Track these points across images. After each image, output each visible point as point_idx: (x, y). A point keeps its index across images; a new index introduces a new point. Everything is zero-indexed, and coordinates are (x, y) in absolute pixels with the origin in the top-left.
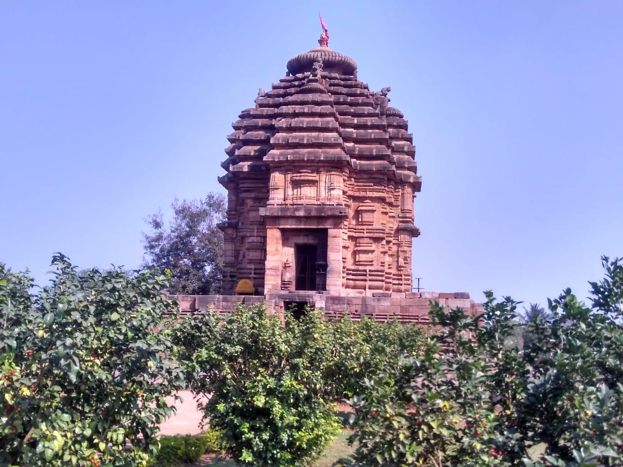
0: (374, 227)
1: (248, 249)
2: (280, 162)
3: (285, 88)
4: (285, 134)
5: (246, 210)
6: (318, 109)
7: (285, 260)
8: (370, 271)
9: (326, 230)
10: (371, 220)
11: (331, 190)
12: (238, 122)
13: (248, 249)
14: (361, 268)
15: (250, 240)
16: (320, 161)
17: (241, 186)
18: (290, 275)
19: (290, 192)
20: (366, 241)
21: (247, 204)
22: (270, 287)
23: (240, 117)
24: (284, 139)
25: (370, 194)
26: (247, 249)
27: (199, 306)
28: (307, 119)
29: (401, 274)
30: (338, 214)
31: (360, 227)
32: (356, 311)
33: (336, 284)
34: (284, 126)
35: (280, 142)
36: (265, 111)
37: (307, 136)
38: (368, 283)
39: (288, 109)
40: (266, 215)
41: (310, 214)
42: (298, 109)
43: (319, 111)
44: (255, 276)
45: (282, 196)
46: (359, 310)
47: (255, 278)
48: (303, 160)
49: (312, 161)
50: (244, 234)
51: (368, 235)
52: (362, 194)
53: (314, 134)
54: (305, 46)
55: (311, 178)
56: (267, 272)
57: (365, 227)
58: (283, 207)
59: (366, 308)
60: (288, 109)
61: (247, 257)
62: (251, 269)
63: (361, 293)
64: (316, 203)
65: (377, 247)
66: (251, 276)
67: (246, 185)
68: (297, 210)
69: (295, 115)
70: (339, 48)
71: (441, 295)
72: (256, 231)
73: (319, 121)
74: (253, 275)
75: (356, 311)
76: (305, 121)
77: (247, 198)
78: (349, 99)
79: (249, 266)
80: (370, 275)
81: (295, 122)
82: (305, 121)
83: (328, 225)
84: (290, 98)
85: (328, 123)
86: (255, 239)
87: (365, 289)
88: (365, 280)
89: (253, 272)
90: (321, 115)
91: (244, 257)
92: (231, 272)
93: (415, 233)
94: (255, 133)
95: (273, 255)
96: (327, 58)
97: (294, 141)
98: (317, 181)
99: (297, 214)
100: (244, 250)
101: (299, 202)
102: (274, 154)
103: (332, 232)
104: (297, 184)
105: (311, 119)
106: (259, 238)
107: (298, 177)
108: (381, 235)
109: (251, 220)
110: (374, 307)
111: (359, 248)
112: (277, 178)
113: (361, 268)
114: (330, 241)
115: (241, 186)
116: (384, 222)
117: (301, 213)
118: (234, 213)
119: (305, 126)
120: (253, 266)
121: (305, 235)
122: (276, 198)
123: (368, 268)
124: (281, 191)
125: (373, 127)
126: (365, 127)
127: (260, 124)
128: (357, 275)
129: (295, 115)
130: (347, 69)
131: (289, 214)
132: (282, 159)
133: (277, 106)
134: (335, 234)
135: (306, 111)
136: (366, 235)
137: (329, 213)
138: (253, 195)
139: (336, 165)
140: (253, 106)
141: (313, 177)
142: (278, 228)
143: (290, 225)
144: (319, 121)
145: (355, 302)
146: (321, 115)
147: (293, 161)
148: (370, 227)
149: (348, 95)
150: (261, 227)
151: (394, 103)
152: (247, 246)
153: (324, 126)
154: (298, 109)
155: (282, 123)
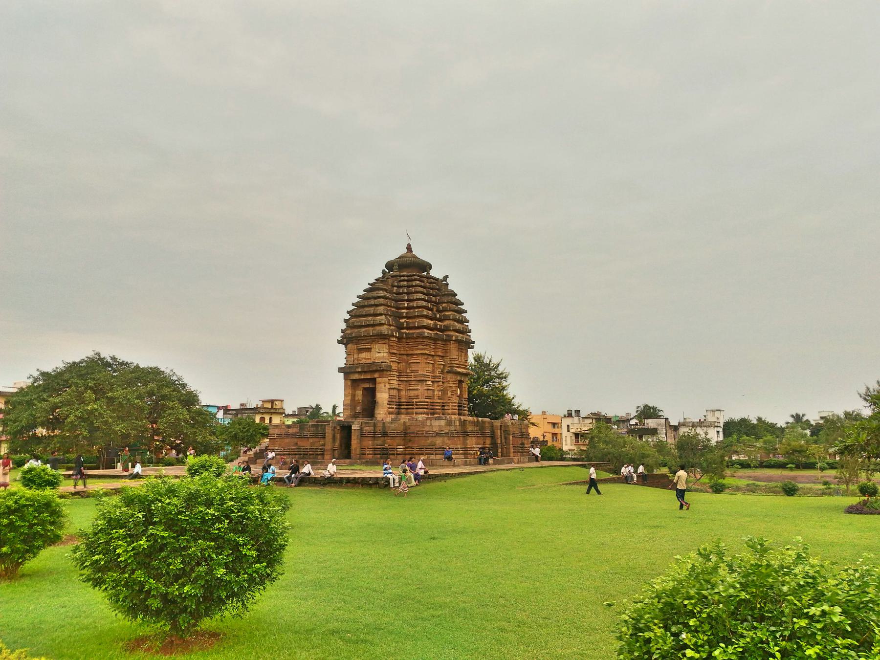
28: (367, 309)
38: (415, 411)
52: (411, 352)
68: (357, 367)
83: (376, 375)
104: (360, 351)
117: (360, 370)
139: (382, 337)
143: (356, 376)
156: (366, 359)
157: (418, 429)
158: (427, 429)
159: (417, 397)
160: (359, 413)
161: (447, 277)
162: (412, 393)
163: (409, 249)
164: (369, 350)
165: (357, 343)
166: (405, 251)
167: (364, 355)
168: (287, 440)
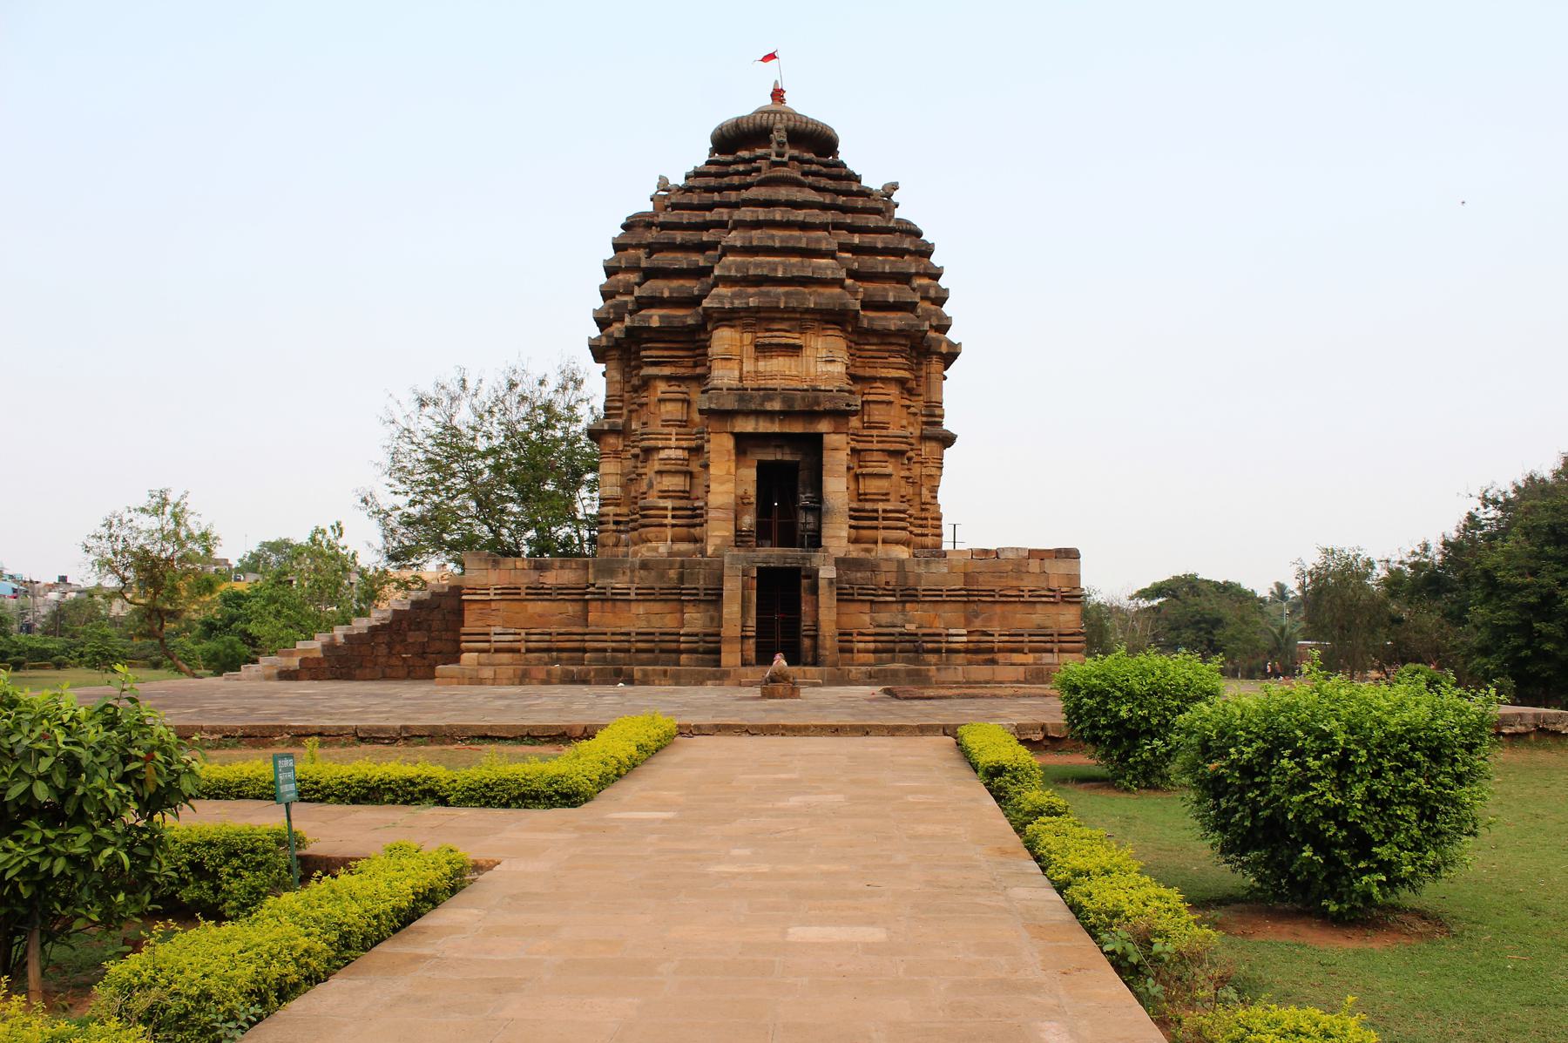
0: (890, 432)
1: (660, 473)
2: (733, 310)
3: (717, 175)
4: (739, 259)
5: (654, 399)
6: (800, 215)
7: (741, 492)
8: (885, 511)
9: (820, 436)
10: (885, 419)
11: (822, 363)
12: (621, 236)
13: (660, 473)
14: (868, 506)
15: (663, 454)
16: (808, 311)
17: (643, 353)
18: (748, 520)
19: (748, 366)
20: (877, 456)
22: (718, 541)
23: (623, 227)
24: (739, 267)
25: (885, 373)
27: (596, 578)
29: (927, 517)
30: (844, 407)
31: (865, 432)
32: (887, 583)
33: (837, 537)
34: (738, 244)
35: (733, 273)
36: (686, 216)
37: (782, 263)
38: (881, 534)
39: (746, 214)
42: (762, 214)
43: (800, 218)
45: (737, 374)
46: (893, 582)
47: (673, 526)
48: (777, 309)
49: (794, 310)
50: (652, 443)
51: (880, 446)
52: (868, 372)
53: (794, 260)
54: (747, 102)
55: (792, 341)
56: (712, 514)
57: (875, 432)
58: (741, 392)
59: (906, 578)
60: (746, 214)
61: (657, 487)
62: (666, 509)
63: (868, 550)
64: (800, 386)
65: (895, 467)
66: (665, 521)
68: (770, 399)
69: (757, 225)
70: (806, 104)
71: (1033, 553)
73: (802, 239)
75: (887, 583)
76: (778, 237)
77: (656, 377)
78: (841, 199)
79: (662, 503)
80: (884, 519)
81: (757, 237)
82: (778, 237)
83: (823, 426)
84: (745, 194)
85: (819, 240)
86: (673, 453)
87: (876, 542)
88: (876, 528)
89: (670, 514)
90: (804, 226)
91: (651, 486)
93: (948, 440)
94: (671, 255)
95: (722, 483)
96: (791, 124)
97: (759, 272)
98: (801, 347)
99: (768, 406)
100: (651, 474)
101: (771, 384)
102: (721, 297)
103: (831, 440)
104: (763, 350)
105: (787, 233)
106: (680, 454)
107: (765, 338)
108: (904, 447)
110: (919, 576)
111: (865, 471)
112: (723, 339)
113: (868, 506)
114: (828, 458)
115: (643, 353)
116: (904, 422)
118: (619, 404)
119: (777, 244)
120: (669, 504)
121: (777, 446)
122: (724, 375)
123: (881, 506)
124: (733, 360)
125: (886, 251)
126: (872, 251)
127: (679, 240)
128: (861, 517)
129: (757, 225)
130: (820, 142)
131: (753, 407)
132: (737, 303)
133: (709, 207)
134: (837, 445)
135: (778, 217)
136: (876, 446)
137: (829, 406)
138: (667, 371)
140: (649, 207)
141: (793, 339)
144: (802, 239)
145: (884, 567)
146: (804, 226)
147: (758, 309)
148: (884, 432)
149: (838, 192)
150: (682, 430)
151: (906, 210)
152: (657, 467)
153: (813, 246)
154: (762, 214)
155: (735, 238)
156: (784, 377)
157: (1004, 582)
158: (1028, 584)
159: (885, 497)
160: (749, 533)
161: (895, 187)
162: (872, 486)
163: (778, 95)
164: (794, 350)
165: (746, 327)
166: (767, 101)
167: (779, 367)
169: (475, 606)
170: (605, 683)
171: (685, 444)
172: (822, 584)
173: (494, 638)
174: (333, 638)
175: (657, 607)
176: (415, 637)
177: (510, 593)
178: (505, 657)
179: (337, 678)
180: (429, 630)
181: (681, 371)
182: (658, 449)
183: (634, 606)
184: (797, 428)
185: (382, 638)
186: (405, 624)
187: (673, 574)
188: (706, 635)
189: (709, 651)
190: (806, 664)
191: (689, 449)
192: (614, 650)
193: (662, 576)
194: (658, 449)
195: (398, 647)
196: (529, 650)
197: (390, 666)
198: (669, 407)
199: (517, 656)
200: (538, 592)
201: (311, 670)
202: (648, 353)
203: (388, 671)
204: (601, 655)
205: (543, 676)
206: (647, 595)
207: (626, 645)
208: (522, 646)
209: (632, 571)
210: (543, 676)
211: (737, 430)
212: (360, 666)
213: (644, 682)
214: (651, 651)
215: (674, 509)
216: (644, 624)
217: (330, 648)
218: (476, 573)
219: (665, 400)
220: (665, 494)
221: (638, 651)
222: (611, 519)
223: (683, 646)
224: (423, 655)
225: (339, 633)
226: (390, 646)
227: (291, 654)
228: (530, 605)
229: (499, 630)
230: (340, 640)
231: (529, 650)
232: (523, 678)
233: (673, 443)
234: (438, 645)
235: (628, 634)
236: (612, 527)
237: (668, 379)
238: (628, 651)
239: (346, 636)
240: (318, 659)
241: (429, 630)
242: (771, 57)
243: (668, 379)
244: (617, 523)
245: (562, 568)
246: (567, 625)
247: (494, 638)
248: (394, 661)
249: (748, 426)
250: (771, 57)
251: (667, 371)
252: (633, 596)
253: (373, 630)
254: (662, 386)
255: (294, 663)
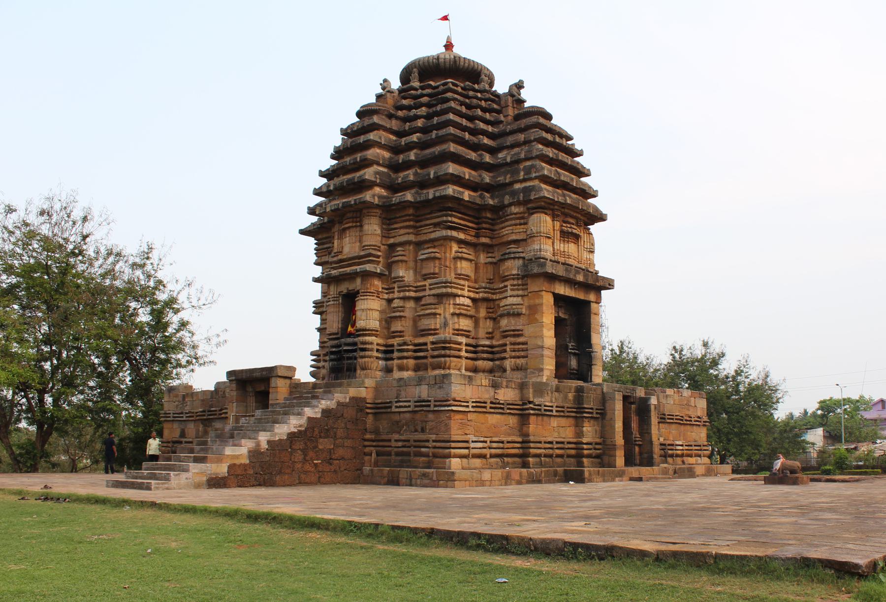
9: (588, 303)
21: (451, 248)
26: (453, 314)
27: (534, 397)
40: (552, 273)
41: (587, 280)
44: (466, 355)
47: (467, 358)
48: (578, 208)
62: (460, 344)
67: (454, 220)
72: (466, 289)
74: (463, 354)
77: (452, 239)
89: (464, 348)
91: (446, 324)
92: (378, 344)
100: (448, 316)
109: (459, 272)
117: (580, 278)
118: (379, 253)
120: (463, 340)
142: (554, 294)
163: (449, 46)
167: (571, 248)
168: (494, 419)
169: (458, 416)
170: (549, 482)
171: (472, 295)
172: (652, 407)
173: (472, 445)
174: (258, 444)
175: (563, 421)
176: (325, 444)
177: (480, 406)
178: (477, 462)
179: (260, 485)
180: (335, 437)
181: (469, 238)
182: (455, 296)
183: (552, 418)
184: (581, 295)
185: (299, 445)
186: (317, 431)
187: (571, 396)
188: (597, 444)
189: (603, 457)
190: (635, 465)
191: (474, 300)
192: (545, 456)
193: (566, 397)
194: (455, 296)
195: (311, 454)
196: (492, 456)
197: (306, 472)
198: (465, 264)
199: (484, 460)
200: (497, 407)
201: (238, 477)
202: (454, 220)
203: (303, 476)
204: (538, 459)
205: (517, 477)
206: (562, 413)
207: (551, 451)
208: (487, 452)
209: (552, 393)
210: (517, 477)
211: (557, 291)
212: (280, 472)
213: (590, 481)
214: (561, 456)
215: (467, 345)
216: (556, 434)
217: (255, 454)
218: (459, 387)
219: (462, 258)
220: (458, 332)
221: (558, 456)
222: (375, 347)
223: (586, 452)
224: (329, 461)
225: (263, 438)
226: (305, 452)
227: (219, 461)
228: (489, 416)
229: (475, 439)
230: (264, 446)
231: (492, 456)
232: (507, 480)
233: (466, 293)
234: (340, 452)
235: (551, 443)
236: (375, 354)
237: (460, 242)
238: (551, 456)
239: (269, 442)
240: (245, 465)
241: (335, 437)
242: (445, 18)
243: (460, 242)
244: (378, 350)
245: (507, 387)
246: (509, 435)
247: (472, 445)
248: (308, 467)
249: (562, 290)
250: (445, 18)
251: (462, 236)
252: (554, 413)
253: (292, 436)
254: (455, 247)
255: (222, 469)
